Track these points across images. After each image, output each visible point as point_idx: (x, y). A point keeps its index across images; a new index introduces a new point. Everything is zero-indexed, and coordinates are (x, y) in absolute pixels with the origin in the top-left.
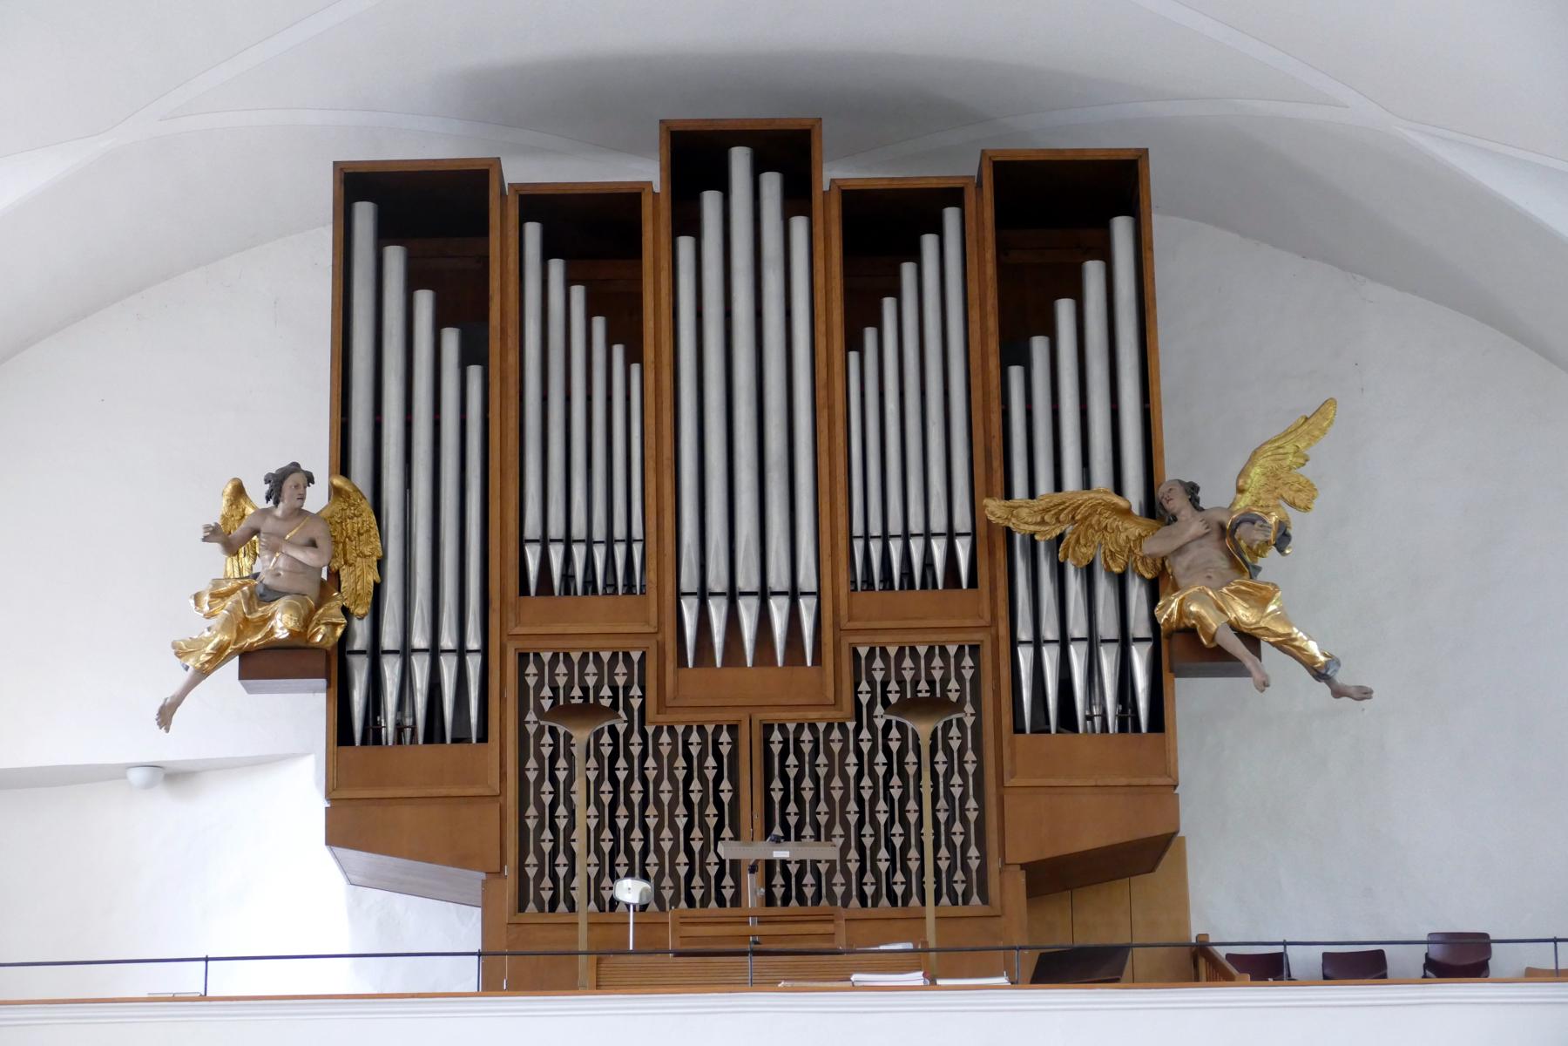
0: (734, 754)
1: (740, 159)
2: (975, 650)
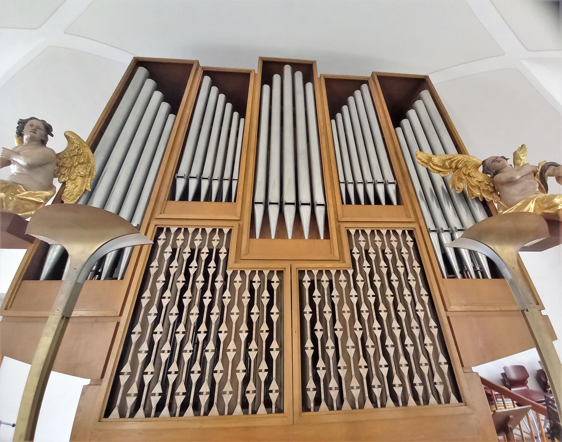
0: (281, 287)
1: (287, 69)
2: (411, 233)
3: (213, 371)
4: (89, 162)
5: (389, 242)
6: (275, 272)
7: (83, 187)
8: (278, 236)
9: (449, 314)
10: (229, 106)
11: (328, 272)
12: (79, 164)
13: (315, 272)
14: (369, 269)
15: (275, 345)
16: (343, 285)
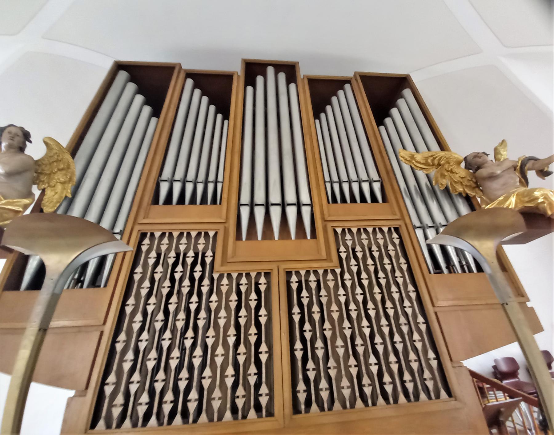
0: (268, 289)
1: (270, 71)
2: (397, 230)
3: (201, 378)
4: (68, 167)
5: (376, 239)
6: (263, 274)
7: (63, 194)
8: (264, 237)
9: (437, 309)
10: (212, 108)
11: (316, 272)
12: (59, 170)
13: (303, 273)
14: (357, 267)
15: (263, 348)
16: (331, 284)
